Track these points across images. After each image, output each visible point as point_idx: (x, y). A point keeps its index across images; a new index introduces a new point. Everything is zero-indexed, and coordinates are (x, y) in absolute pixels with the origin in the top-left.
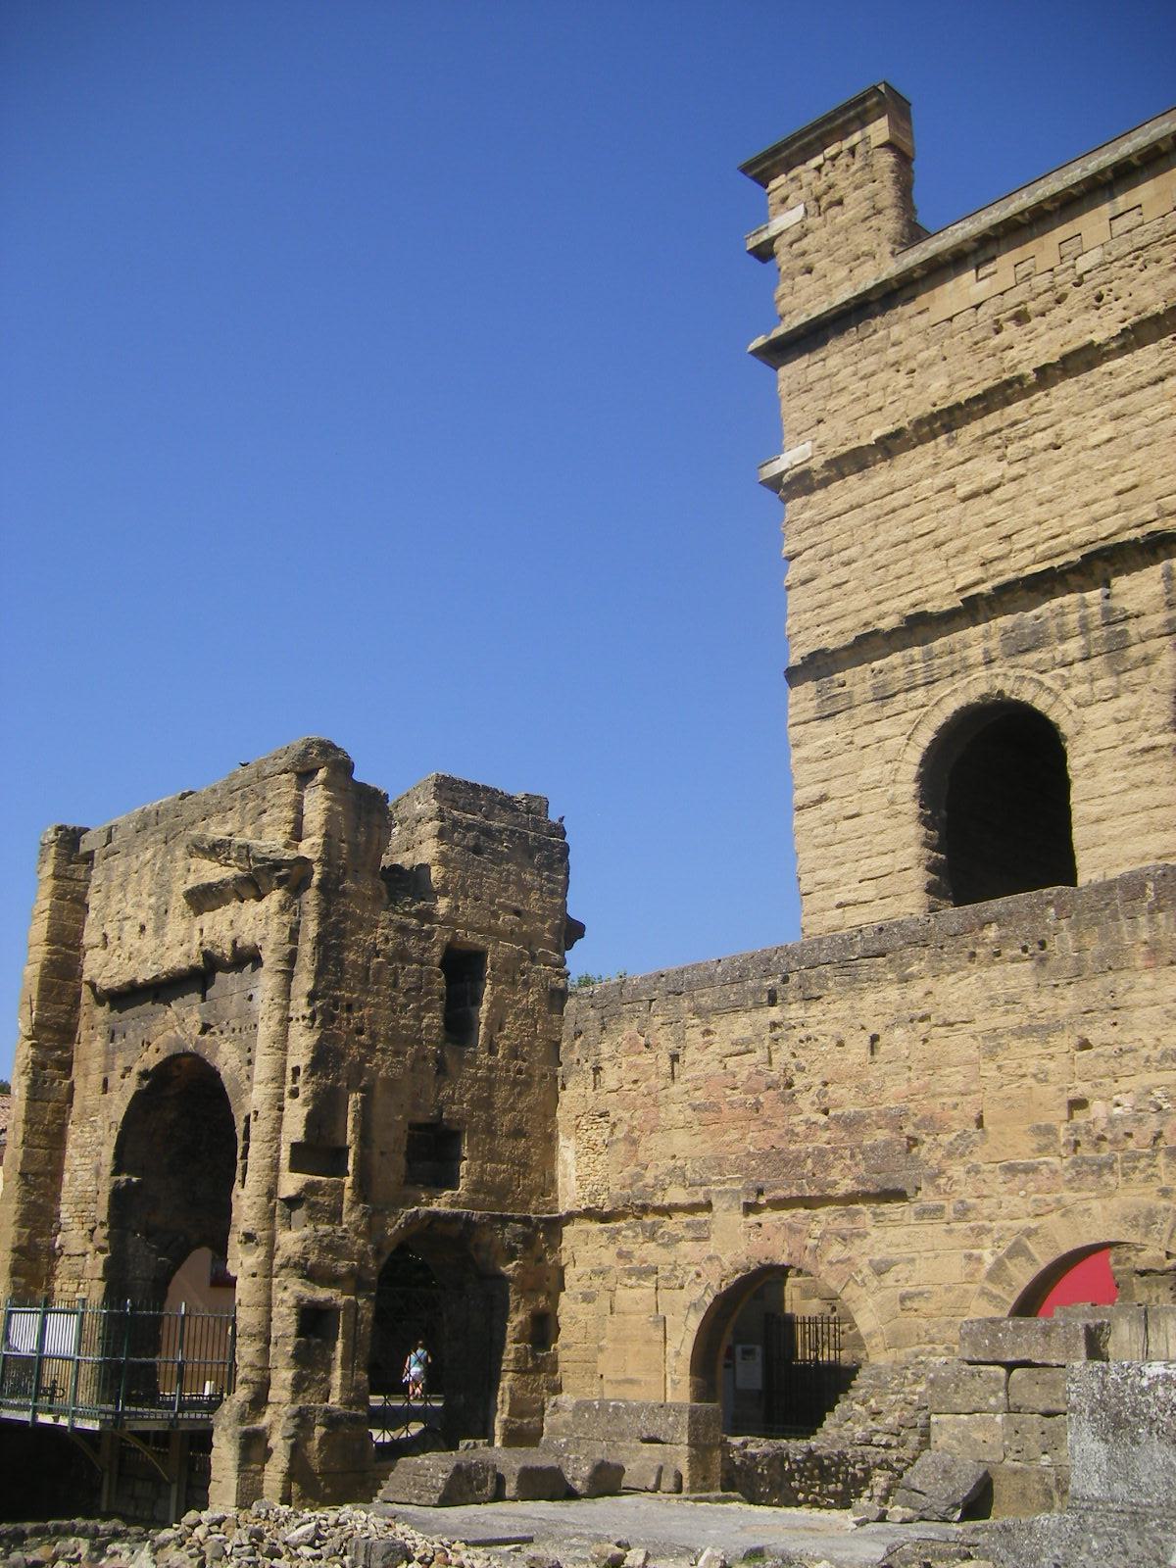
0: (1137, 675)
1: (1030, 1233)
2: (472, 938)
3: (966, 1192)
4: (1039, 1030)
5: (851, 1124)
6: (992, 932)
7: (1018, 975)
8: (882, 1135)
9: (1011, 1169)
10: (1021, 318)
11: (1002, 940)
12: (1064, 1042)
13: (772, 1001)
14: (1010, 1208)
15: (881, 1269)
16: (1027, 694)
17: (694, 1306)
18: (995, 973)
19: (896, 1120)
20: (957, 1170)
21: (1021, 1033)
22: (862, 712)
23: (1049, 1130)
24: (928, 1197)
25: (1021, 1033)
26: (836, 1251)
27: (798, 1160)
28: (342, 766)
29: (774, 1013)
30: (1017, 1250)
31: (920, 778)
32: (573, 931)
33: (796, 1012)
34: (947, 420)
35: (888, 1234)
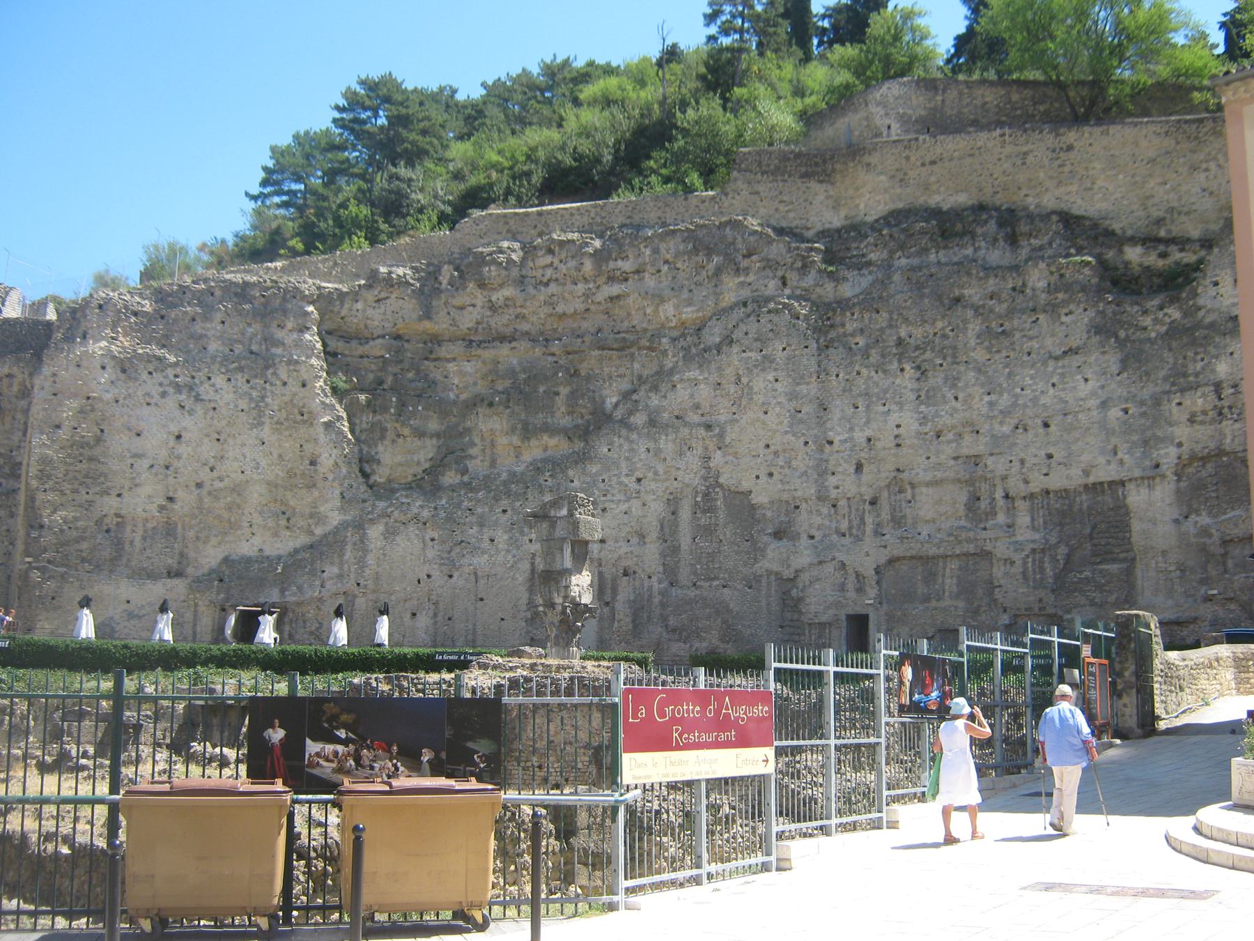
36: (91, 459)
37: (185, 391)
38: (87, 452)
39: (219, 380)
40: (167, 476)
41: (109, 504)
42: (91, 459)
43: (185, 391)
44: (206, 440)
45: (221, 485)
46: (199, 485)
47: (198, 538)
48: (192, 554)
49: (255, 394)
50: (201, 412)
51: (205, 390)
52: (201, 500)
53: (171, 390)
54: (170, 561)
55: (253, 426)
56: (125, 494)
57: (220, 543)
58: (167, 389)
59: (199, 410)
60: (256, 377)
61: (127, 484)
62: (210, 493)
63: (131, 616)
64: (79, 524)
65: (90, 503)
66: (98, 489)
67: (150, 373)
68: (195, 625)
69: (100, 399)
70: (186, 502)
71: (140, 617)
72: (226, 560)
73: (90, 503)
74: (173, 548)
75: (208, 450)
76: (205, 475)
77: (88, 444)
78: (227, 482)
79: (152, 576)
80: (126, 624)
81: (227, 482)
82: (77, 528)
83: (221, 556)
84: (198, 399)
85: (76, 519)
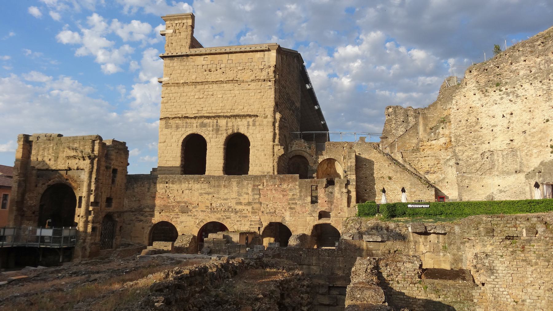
0: (220, 136)
1: (204, 219)
2: (116, 168)
3: (195, 213)
4: (208, 194)
5: (178, 202)
6: (203, 179)
7: (206, 186)
8: (183, 204)
9: (202, 211)
10: (210, 71)
11: (204, 181)
12: (210, 196)
13: (167, 183)
14: (201, 216)
15: (181, 222)
16: (202, 134)
17: (150, 226)
18: (202, 185)
19: (185, 203)
20: (194, 210)
21: (205, 193)
22: (173, 129)
23: (208, 206)
24: (190, 213)
25: (205, 193)
26: (174, 220)
27: (169, 206)
28: (100, 138)
29: (167, 185)
30: (201, 221)
31: (182, 143)
32: (128, 164)
33: (171, 185)
34: (195, 83)
35: (183, 218)
36: (475, 131)
37: (511, 95)
38: (473, 129)
39: (527, 86)
40: (508, 131)
41: (485, 147)
42: (475, 131)
43: (511, 95)
44: (524, 113)
45: (534, 130)
46: (524, 132)
47: (527, 155)
48: (525, 162)
49: (544, 87)
50: (520, 102)
51: (520, 92)
52: (526, 139)
53: (505, 96)
54: (516, 167)
55: (546, 101)
56: (491, 141)
57: (538, 156)
58: (503, 96)
59: (519, 100)
60: (544, 79)
61: (492, 138)
62: (529, 135)
63: (501, 191)
64: (474, 157)
65: (477, 148)
66: (479, 142)
67: (495, 91)
68: (531, 193)
69: (475, 107)
70: (519, 140)
71: (505, 192)
72: (542, 163)
73: (477, 148)
74: (516, 161)
75: (526, 116)
76: (526, 127)
77: (473, 125)
78: (537, 128)
79: (508, 173)
80: (499, 195)
81: (537, 128)
82: (473, 159)
83: (539, 162)
84: (517, 96)
85: (473, 155)
